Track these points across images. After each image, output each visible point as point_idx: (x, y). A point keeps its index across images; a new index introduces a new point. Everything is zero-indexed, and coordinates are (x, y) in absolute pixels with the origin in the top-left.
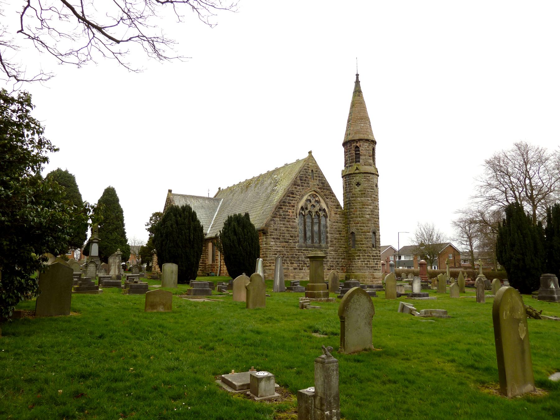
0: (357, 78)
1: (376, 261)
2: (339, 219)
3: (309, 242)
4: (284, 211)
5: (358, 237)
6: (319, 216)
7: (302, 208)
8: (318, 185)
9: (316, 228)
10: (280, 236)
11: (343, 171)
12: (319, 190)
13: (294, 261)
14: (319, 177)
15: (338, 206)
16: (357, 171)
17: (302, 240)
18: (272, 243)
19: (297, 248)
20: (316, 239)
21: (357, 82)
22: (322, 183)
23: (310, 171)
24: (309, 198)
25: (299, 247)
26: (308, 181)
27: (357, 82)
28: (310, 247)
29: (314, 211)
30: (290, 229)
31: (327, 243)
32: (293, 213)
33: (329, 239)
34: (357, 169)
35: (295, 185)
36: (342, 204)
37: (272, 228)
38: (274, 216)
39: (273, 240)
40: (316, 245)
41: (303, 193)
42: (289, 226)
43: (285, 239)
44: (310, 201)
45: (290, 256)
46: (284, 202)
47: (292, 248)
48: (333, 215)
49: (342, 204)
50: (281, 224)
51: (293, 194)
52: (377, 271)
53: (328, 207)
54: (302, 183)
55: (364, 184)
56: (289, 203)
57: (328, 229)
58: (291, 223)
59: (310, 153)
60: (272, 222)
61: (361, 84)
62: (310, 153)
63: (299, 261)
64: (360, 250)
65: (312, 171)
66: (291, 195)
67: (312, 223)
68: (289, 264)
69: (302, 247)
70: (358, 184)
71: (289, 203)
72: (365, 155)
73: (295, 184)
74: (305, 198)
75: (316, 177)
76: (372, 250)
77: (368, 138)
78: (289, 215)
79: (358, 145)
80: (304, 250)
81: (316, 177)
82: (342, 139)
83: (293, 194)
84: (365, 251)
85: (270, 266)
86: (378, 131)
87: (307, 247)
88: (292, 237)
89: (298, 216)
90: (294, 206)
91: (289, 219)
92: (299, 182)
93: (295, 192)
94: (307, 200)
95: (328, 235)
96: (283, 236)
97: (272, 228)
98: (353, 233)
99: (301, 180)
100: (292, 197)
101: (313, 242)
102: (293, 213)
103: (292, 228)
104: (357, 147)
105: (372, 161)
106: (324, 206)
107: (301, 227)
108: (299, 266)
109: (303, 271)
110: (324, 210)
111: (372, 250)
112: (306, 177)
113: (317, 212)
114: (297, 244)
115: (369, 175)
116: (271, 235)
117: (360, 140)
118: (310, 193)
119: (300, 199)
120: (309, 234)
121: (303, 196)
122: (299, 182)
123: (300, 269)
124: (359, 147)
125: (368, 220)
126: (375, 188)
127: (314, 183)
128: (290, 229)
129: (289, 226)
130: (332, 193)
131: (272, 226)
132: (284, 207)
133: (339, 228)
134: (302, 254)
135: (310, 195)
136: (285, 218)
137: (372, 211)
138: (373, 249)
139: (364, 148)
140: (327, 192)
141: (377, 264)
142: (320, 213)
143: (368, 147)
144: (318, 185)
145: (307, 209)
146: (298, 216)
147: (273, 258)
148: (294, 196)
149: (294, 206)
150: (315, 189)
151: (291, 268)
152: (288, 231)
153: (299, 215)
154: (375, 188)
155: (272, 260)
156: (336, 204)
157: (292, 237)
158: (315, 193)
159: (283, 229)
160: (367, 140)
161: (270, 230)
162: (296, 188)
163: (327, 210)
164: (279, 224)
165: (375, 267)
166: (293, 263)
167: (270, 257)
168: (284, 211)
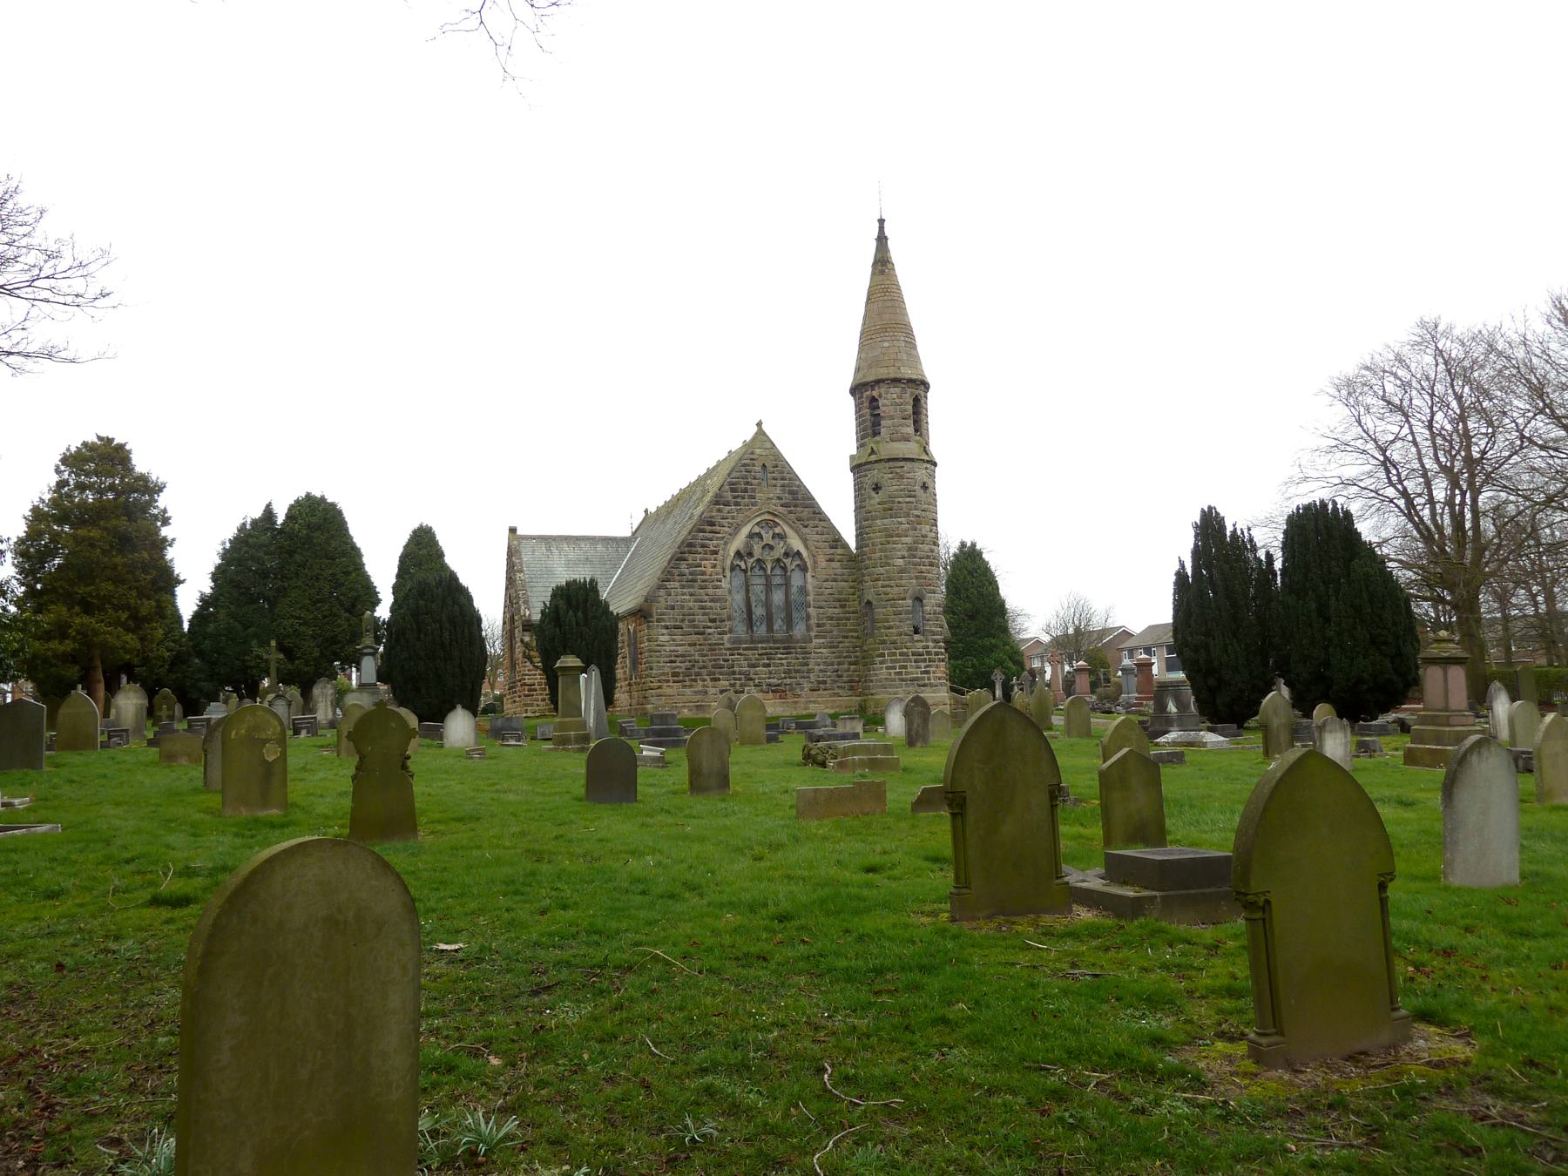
0: (881, 228)
2: (839, 571)
3: (761, 630)
4: (690, 566)
5: (879, 612)
6: (784, 569)
7: (738, 554)
9: (778, 597)
11: (852, 457)
12: (781, 509)
15: (837, 541)
16: (873, 458)
17: (741, 630)
18: (662, 638)
20: (778, 624)
21: (882, 240)
22: (791, 492)
23: (758, 468)
24: (757, 530)
27: (882, 240)
29: (769, 558)
31: (809, 628)
32: (714, 566)
33: (813, 621)
34: (873, 452)
35: (717, 503)
36: (849, 534)
38: (666, 577)
40: (778, 636)
41: (738, 521)
44: (759, 535)
46: (690, 545)
47: (713, 647)
48: (824, 564)
49: (849, 534)
51: (712, 524)
52: (928, 689)
53: (807, 547)
55: (891, 487)
56: (703, 546)
57: (810, 598)
58: (710, 591)
59: (759, 424)
60: (662, 592)
62: (759, 424)
64: (884, 642)
66: (708, 528)
67: (768, 587)
69: (740, 642)
70: (877, 488)
71: (703, 546)
72: (892, 418)
73: (718, 501)
74: (745, 531)
76: (913, 641)
78: (703, 573)
79: (875, 394)
82: (848, 379)
83: (712, 524)
84: (894, 642)
86: (935, 357)
89: (728, 573)
90: (716, 553)
92: (729, 496)
93: (718, 519)
94: (751, 536)
95: (810, 610)
98: (869, 603)
99: (733, 490)
101: (770, 628)
102: (714, 566)
104: (873, 400)
105: (911, 430)
106: (796, 544)
107: (739, 598)
110: (798, 553)
111: (913, 641)
113: (778, 560)
114: (726, 637)
117: (878, 382)
119: (733, 535)
120: (759, 611)
121: (738, 528)
122: (729, 496)
124: (889, 397)
125: (902, 571)
126: (920, 492)
127: (768, 496)
130: (818, 515)
132: (690, 557)
133: (840, 593)
136: (694, 581)
137: (910, 549)
138: (916, 637)
139: (890, 399)
140: (806, 513)
141: (927, 672)
142: (788, 561)
145: (750, 554)
146: (728, 573)
148: (717, 528)
149: (716, 553)
150: (772, 508)
151: (712, 691)
153: (732, 569)
154: (920, 492)
156: (830, 537)
160: (896, 381)
161: (656, 610)
163: (805, 553)
164: (679, 594)
168: (690, 566)
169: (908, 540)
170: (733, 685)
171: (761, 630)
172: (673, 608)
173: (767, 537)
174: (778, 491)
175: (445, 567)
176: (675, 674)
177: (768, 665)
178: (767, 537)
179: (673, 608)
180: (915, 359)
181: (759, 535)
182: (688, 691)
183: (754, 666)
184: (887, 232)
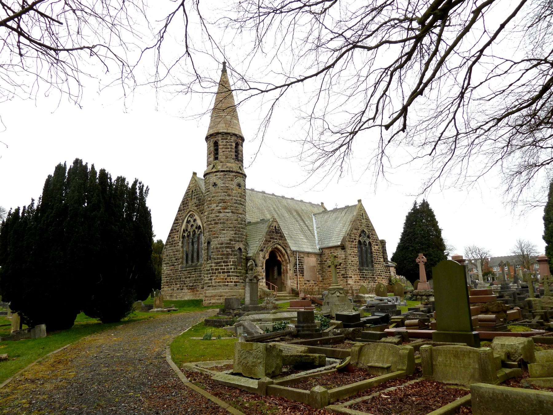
1: (209, 275)
3: (190, 263)
7: (184, 231)
12: (195, 208)
18: (165, 268)
19: (180, 270)
22: (199, 200)
52: (211, 288)
68: (175, 286)
87: (186, 267)
89: (181, 239)
106: (199, 223)
108: (180, 286)
109: (183, 291)
136: (172, 244)
141: (211, 279)
145: (187, 230)
149: (178, 231)
151: (175, 289)
152: (174, 255)
153: (183, 237)
157: (176, 259)
165: (208, 283)
169: (206, 214)
171: (190, 263)
178: (192, 221)
183: (186, 278)
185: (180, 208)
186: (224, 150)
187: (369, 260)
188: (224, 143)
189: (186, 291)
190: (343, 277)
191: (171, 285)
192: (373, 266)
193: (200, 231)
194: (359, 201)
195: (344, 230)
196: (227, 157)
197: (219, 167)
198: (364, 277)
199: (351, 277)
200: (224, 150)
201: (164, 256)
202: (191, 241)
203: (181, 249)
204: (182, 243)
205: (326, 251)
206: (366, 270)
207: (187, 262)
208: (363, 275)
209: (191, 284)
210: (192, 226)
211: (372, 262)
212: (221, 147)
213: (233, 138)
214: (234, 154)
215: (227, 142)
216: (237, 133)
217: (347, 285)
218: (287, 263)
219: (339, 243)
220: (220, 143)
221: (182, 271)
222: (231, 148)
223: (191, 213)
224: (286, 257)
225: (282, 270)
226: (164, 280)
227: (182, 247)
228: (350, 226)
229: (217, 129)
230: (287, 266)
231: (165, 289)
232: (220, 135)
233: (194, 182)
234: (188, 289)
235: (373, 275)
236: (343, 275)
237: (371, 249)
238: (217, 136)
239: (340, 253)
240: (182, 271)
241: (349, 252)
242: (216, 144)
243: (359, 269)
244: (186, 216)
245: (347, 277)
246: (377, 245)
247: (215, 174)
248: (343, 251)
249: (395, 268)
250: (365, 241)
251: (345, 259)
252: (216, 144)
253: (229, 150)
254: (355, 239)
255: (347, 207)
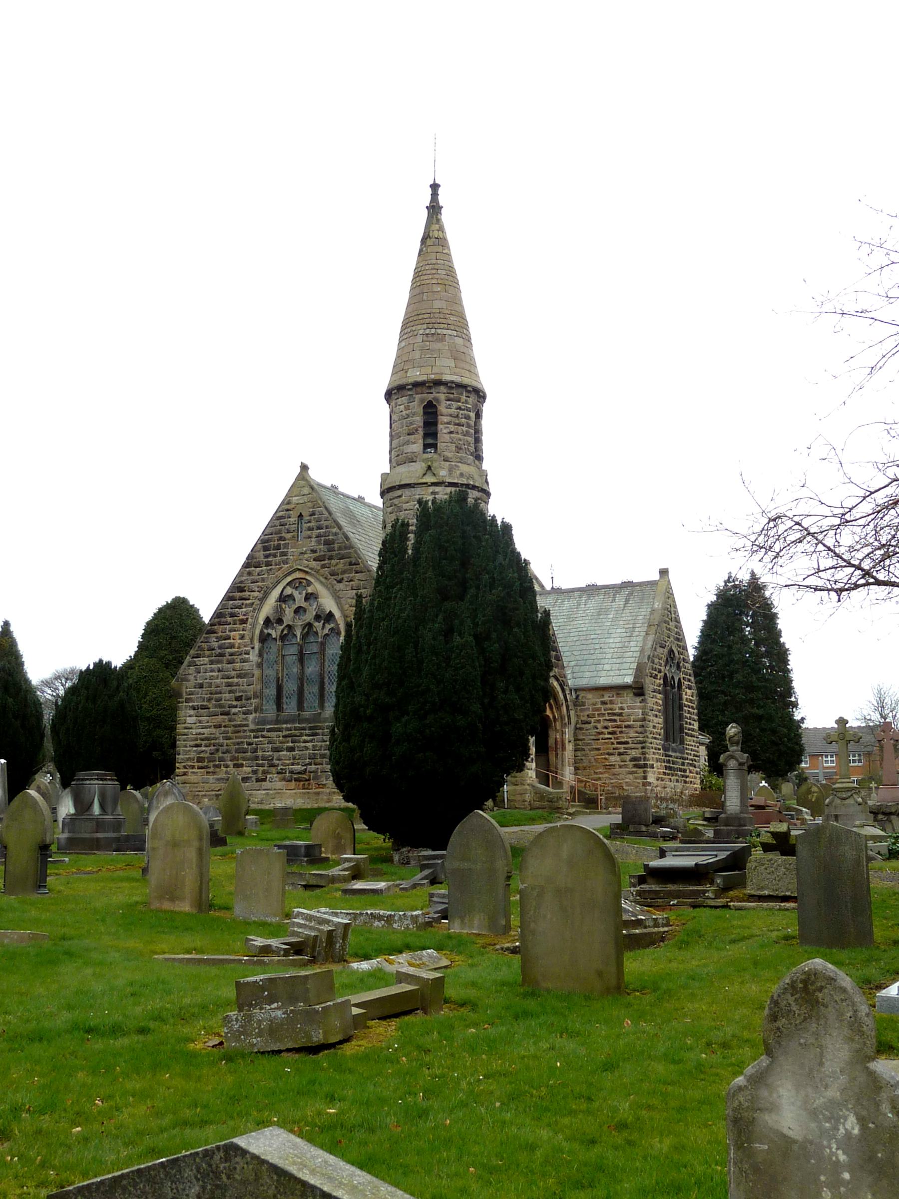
3: (291, 707)
7: (267, 622)
8: (314, 551)
10: (209, 700)
12: (314, 564)
13: (244, 759)
14: (319, 528)
18: (189, 720)
19: (252, 727)
22: (328, 543)
24: (289, 591)
25: (258, 724)
26: (286, 546)
28: (286, 722)
30: (236, 680)
37: (192, 682)
39: (192, 712)
41: (268, 583)
42: (233, 673)
43: (221, 706)
45: (234, 748)
50: (212, 671)
54: (266, 556)
58: (238, 665)
61: (446, 217)
63: (257, 758)
65: (301, 516)
66: (238, 594)
68: (231, 769)
75: (310, 529)
77: (403, 381)
78: (232, 646)
80: (269, 730)
81: (310, 529)
83: (241, 590)
85: (185, 774)
87: (277, 722)
88: (238, 699)
89: (257, 645)
91: (231, 654)
94: (283, 599)
96: (218, 700)
97: (192, 682)
99: (265, 549)
100: (242, 599)
101: (300, 706)
102: (242, 637)
103: (239, 676)
105: (417, 447)
112: (281, 539)
113: (310, 625)
114: (251, 717)
115: (399, 493)
116: (187, 701)
118: (289, 579)
119: (263, 600)
122: (261, 555)
123: (258, 780)
128: (236, 680)
129: (233, 673)
131: (191, 678)
134: (266, 740)
135: (289, 584)
140: (341, 565)
142: (318, 625)
143: (407, 408)
144: (314, 551)
145: (280, 621)
147: (192, 755)
149: (244, 622)
152: (229, 685)
153: (264, 639)
155: (189, 759)
157: (238, 699)
158: (301, 575)
159: (218, 681)
162: (249, 574)
163: (337, 614)
166: (242, 766)
167: (187, 752)
168: (219, 639)
170: (255, 772)
171: (291, 707)
172: (201, 686)
173: (299, 597)
174: (313, 543)
175: (137, 654)
176: (200, 760)
177: (291, 749)
178: (299, 597)
179: (201, 686)
180: (463, 356)
181: (291, 597)
182: (211, 778)
183: (276, 750)
184: (442, 200)
185: (250, 557)
186: (452, 428)
187: (677, 726)
188: (453, 411)
189: (280, 784)
190: (635, 766)
191: (219, 766)
192: (682, 742)
193: (328, 627)
194: (664, 572)
195: (635, 646)
196: (459, 449)
197: (443, 473)
198: (670, 768)
199: (652, 767)
200: (452, 428)
201: (187, 688)
202: (294, 650)
203: (257, 672)
204: (260, 655)
205: (590, 696)
206: (674, 751)
207: (279, 708)
208: (669, 762)
209: (298, 768)
210: (298, 610)
211: (681, 729)
212: (445, 419)
213: (472, 399)
214: (471, 440)
215: (459, 408)
216: (466, 381)
217: (644, 784)
218: (564, 725)
219: (629, 680)
220: (442, 408)
221: (263, 730)
222: (469, 426)
223: (298, 575)
224: (564, 708)
225: (551, 742)
226: (185, 752)
227: (260, 665)
228: (651, 638)
229: (435, 370)
230: (563, 733)
231: (192, 778)
232: (442, 389)
233: (306, 490)
234: (284, 779)
235: (683, 764)
236: (634, 759)
237: (681, 698)
238: (433, 390)
239: (629, 705)
240: (263, 730)
241: (651, 702)
242: (431, 411)
243: (666, 749)
244: (278, 582)
245: (645, 766)
246: (690, 689)
247: (431, 489)
248: (639, 699)
249: (708, 747)
250: (673, 677)
251: (644, 720)
252: (431, 411)
253: (465, 429)
254: (660, 672)
255: (627, 585)
